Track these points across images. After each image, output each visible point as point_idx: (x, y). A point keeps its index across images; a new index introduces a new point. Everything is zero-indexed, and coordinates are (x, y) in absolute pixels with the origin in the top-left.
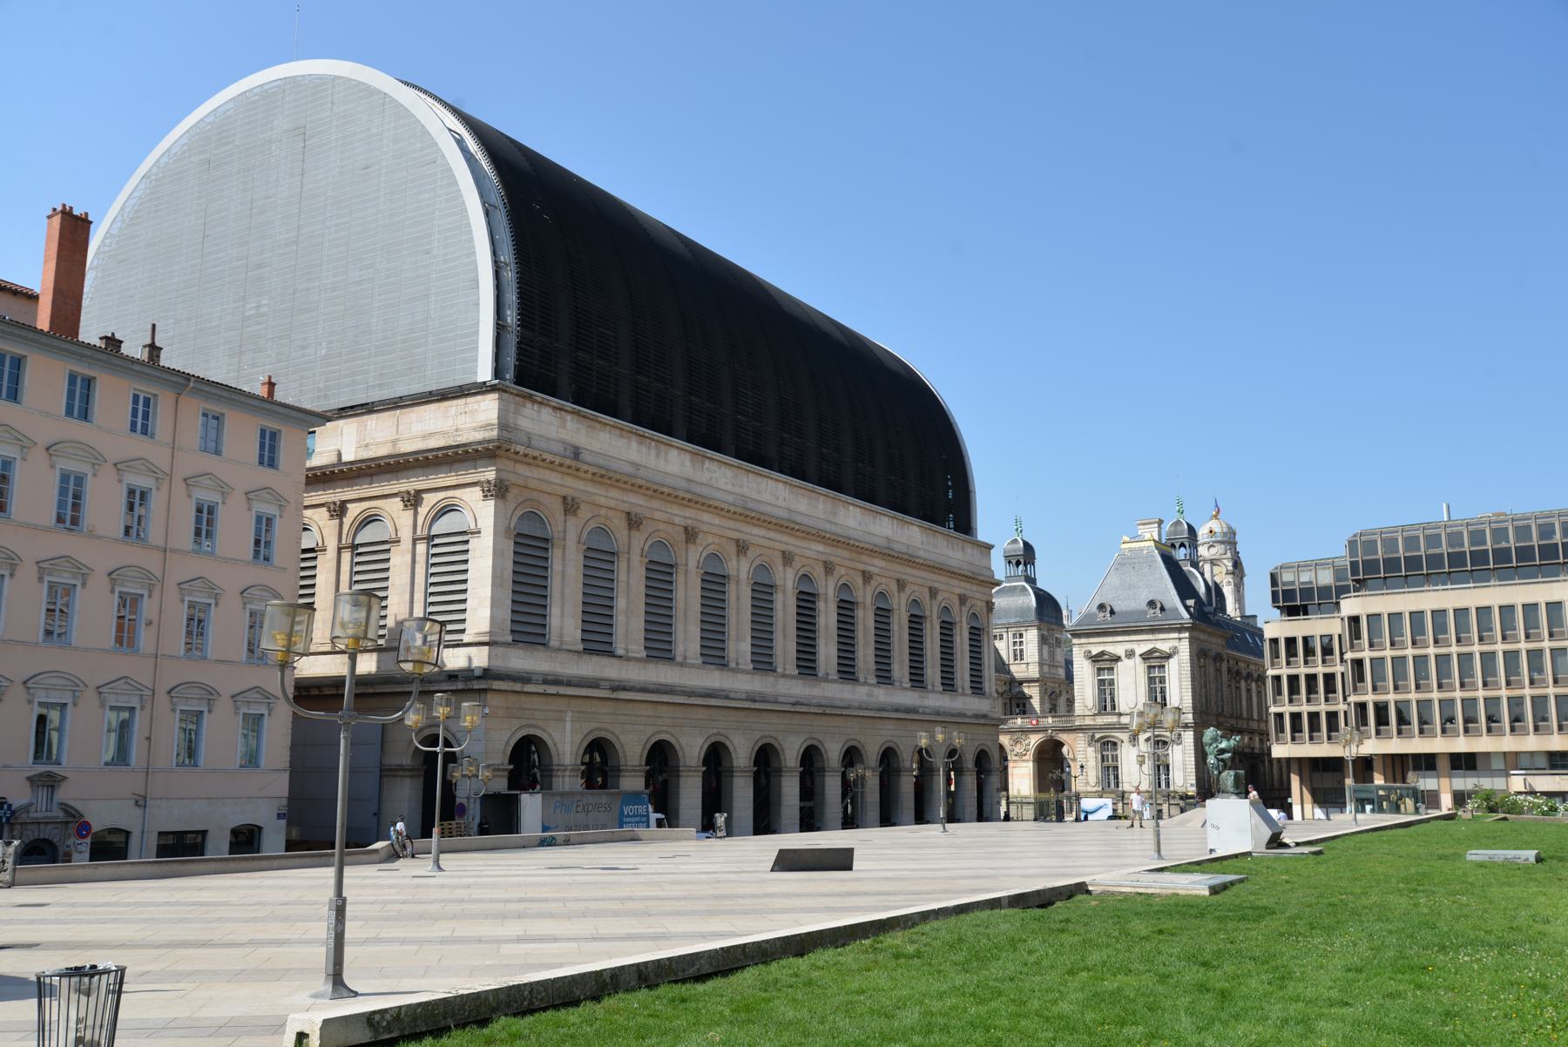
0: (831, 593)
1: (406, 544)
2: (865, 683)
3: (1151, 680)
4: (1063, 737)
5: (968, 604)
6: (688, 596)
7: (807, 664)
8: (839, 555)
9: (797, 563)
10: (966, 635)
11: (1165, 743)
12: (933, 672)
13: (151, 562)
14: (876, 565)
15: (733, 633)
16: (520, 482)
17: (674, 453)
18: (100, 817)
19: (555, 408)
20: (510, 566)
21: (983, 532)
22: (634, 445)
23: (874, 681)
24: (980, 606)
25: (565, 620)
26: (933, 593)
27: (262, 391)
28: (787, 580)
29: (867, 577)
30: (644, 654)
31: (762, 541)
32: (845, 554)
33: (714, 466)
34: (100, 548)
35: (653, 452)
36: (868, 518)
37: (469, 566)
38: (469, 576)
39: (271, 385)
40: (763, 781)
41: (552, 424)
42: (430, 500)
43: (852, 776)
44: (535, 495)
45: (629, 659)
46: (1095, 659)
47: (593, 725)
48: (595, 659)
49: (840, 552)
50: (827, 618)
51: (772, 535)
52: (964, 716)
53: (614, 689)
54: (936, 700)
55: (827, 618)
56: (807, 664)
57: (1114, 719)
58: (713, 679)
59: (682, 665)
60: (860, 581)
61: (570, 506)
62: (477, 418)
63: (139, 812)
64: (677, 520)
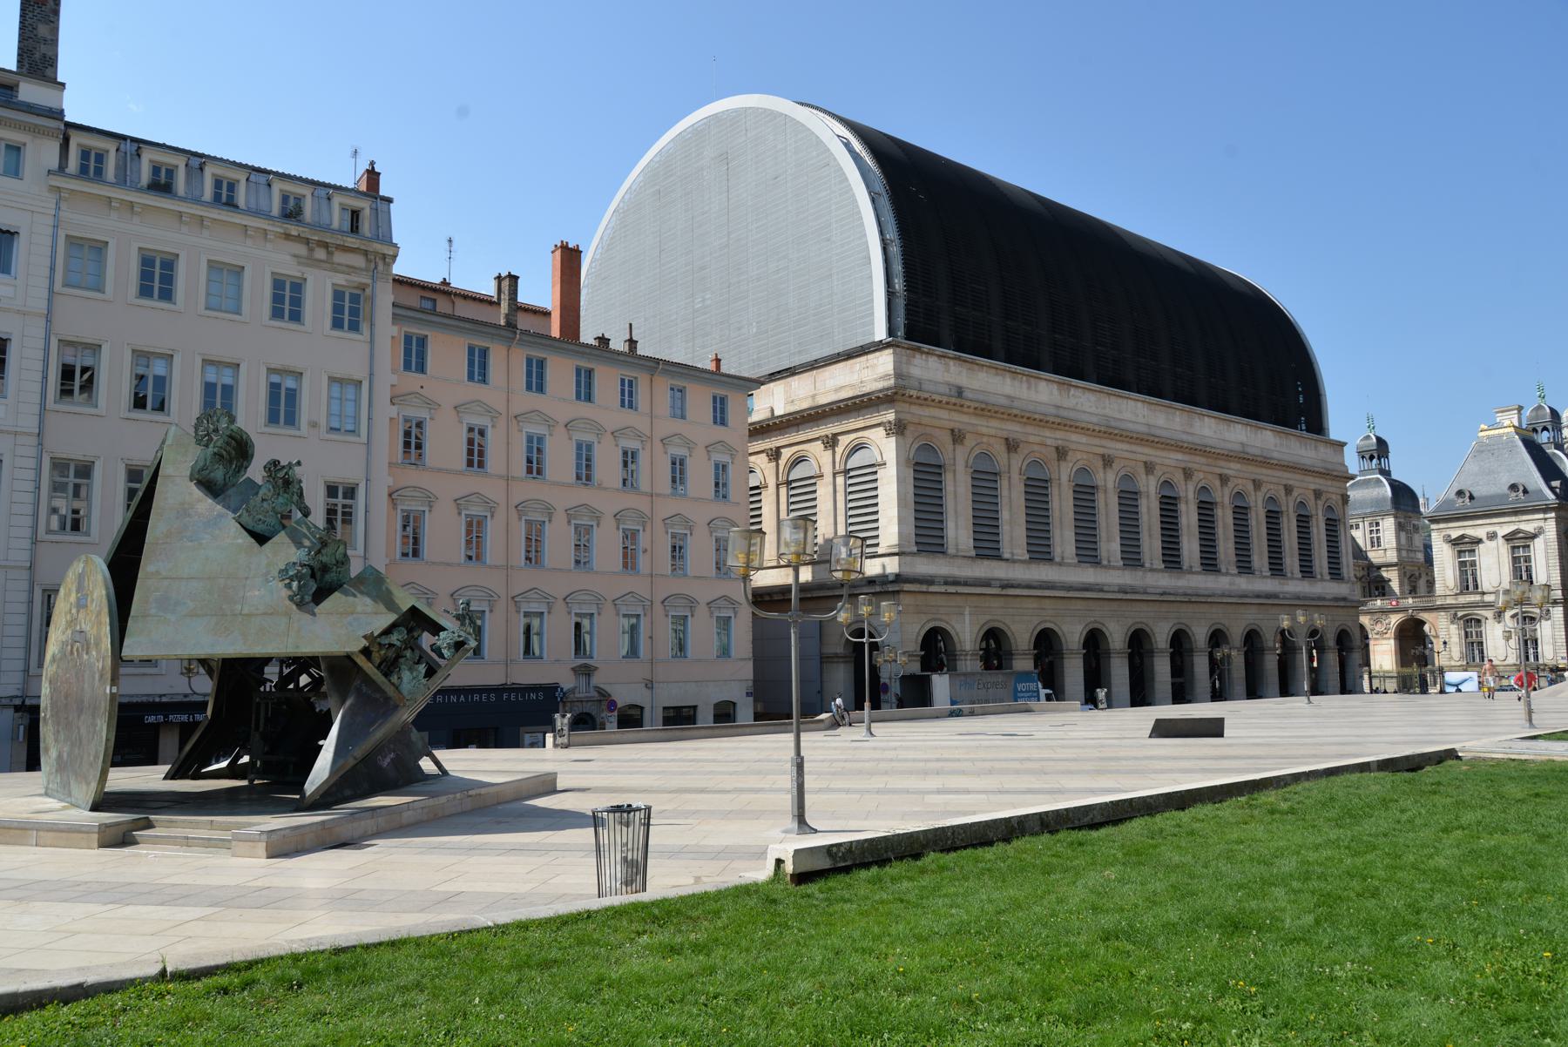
0: (1191, 495)
1: (828, 478)
2: (1227, 574)
3: (1515, 560)
4: (1424, 616)
5: (1323, 498)
6: (1062, 505)
7: (1172, 559)
8: (1197, 462)
9: (1158, 472)
10: (1323, 526)
11: (1532, 619)
12: (1291, 561)
13: (642, 504)
14: (1232, 468)
15: (1103, 535)
17: (1042, 385)
18: (624, 696)
20: (911, 490)
21: (1335, 430)
22: (1008, 380)
23: (1235, 571)
24: (1335, 499)
25: (959, 530)
26: (1288, 490)
27: (711, 366)
28: (1150, 488)
29: (1224, 479)
30: (1027, 557)
32: (1203, 460)
33: (1079, 393)
34: (607, 498)
35: (1025, 386)
36: (1223, 426)
37: (879, 492)
38: (879, 500)
39: (718, 361)
40: (1137, 660)
41: (938, 370)
42: (844, 441)
43: (1218, 655)
44: (928, 430)
45: (1014, 561)
46: (1455, 542)
47: (988, 617)
48: (986, 562)
49: (1198, 459)
50: (1189, 518)
51: (1134, 448)
52: (1324, 599)
53: (1003, 587)
54: (1296, 586)
55: (1189, 518)
56: (1172, 559)
57: (1477, 598)
58: (1088, 575)
59: (1060, 564)
60: (1217, 483)
61: (957, 437)
62: (877, 371)
63: (648, 692)
64: (1049, 442)
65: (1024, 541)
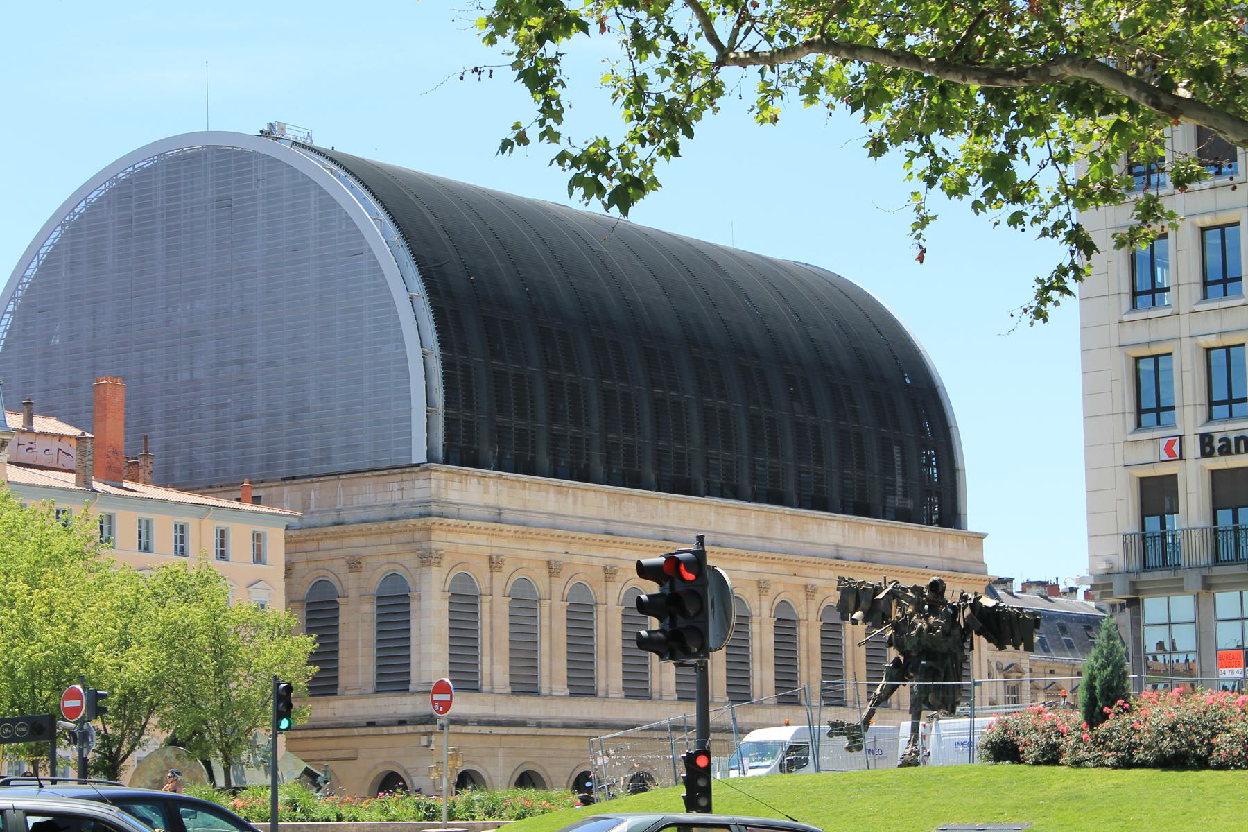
17: (591, 495)
22: (552, 495)
48: (523, 700)
49: (776, 568)
53: (539, 725)
64: (596, 562)
65: (565, 674)
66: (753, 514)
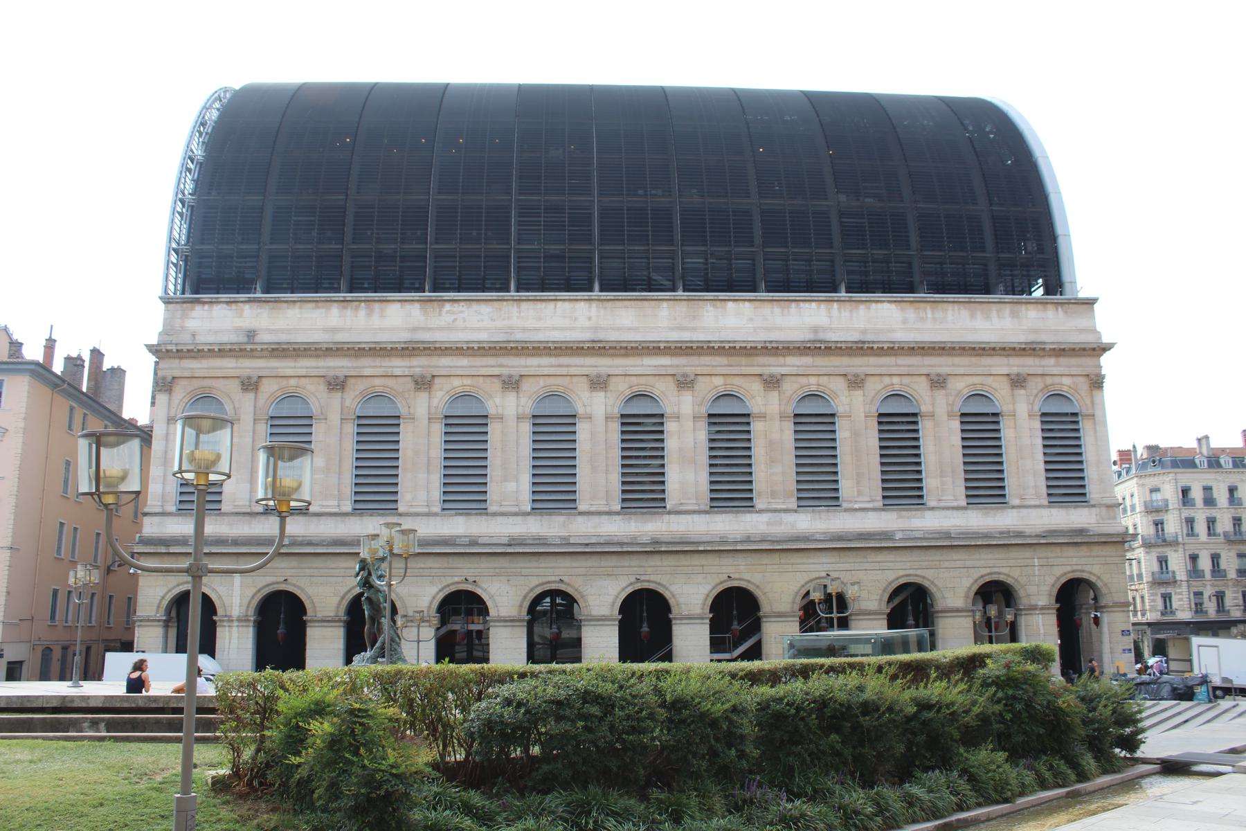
16: (186, 374)
19: (227, 303)
31: (546, 371)
33: (457, 307)
44: (207, 382)
64: (398, 372)
66: (665, 304)
